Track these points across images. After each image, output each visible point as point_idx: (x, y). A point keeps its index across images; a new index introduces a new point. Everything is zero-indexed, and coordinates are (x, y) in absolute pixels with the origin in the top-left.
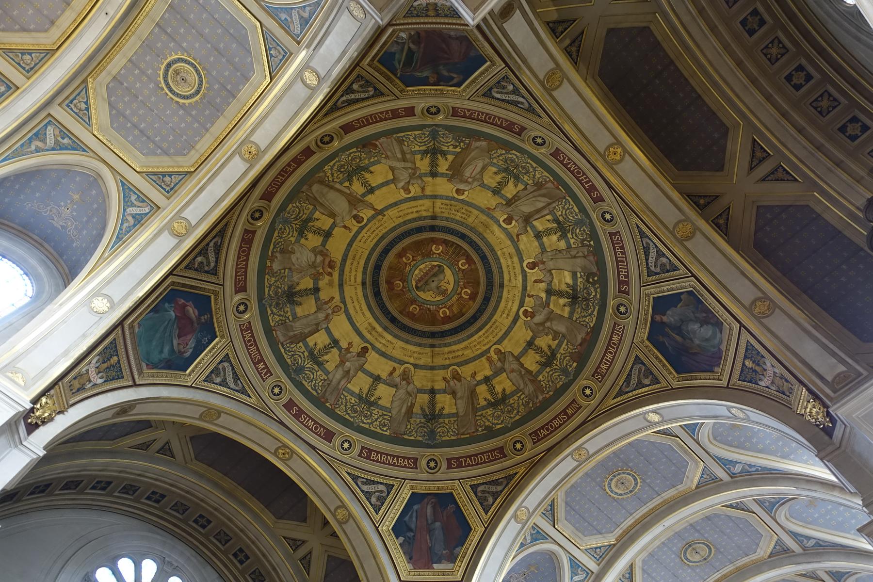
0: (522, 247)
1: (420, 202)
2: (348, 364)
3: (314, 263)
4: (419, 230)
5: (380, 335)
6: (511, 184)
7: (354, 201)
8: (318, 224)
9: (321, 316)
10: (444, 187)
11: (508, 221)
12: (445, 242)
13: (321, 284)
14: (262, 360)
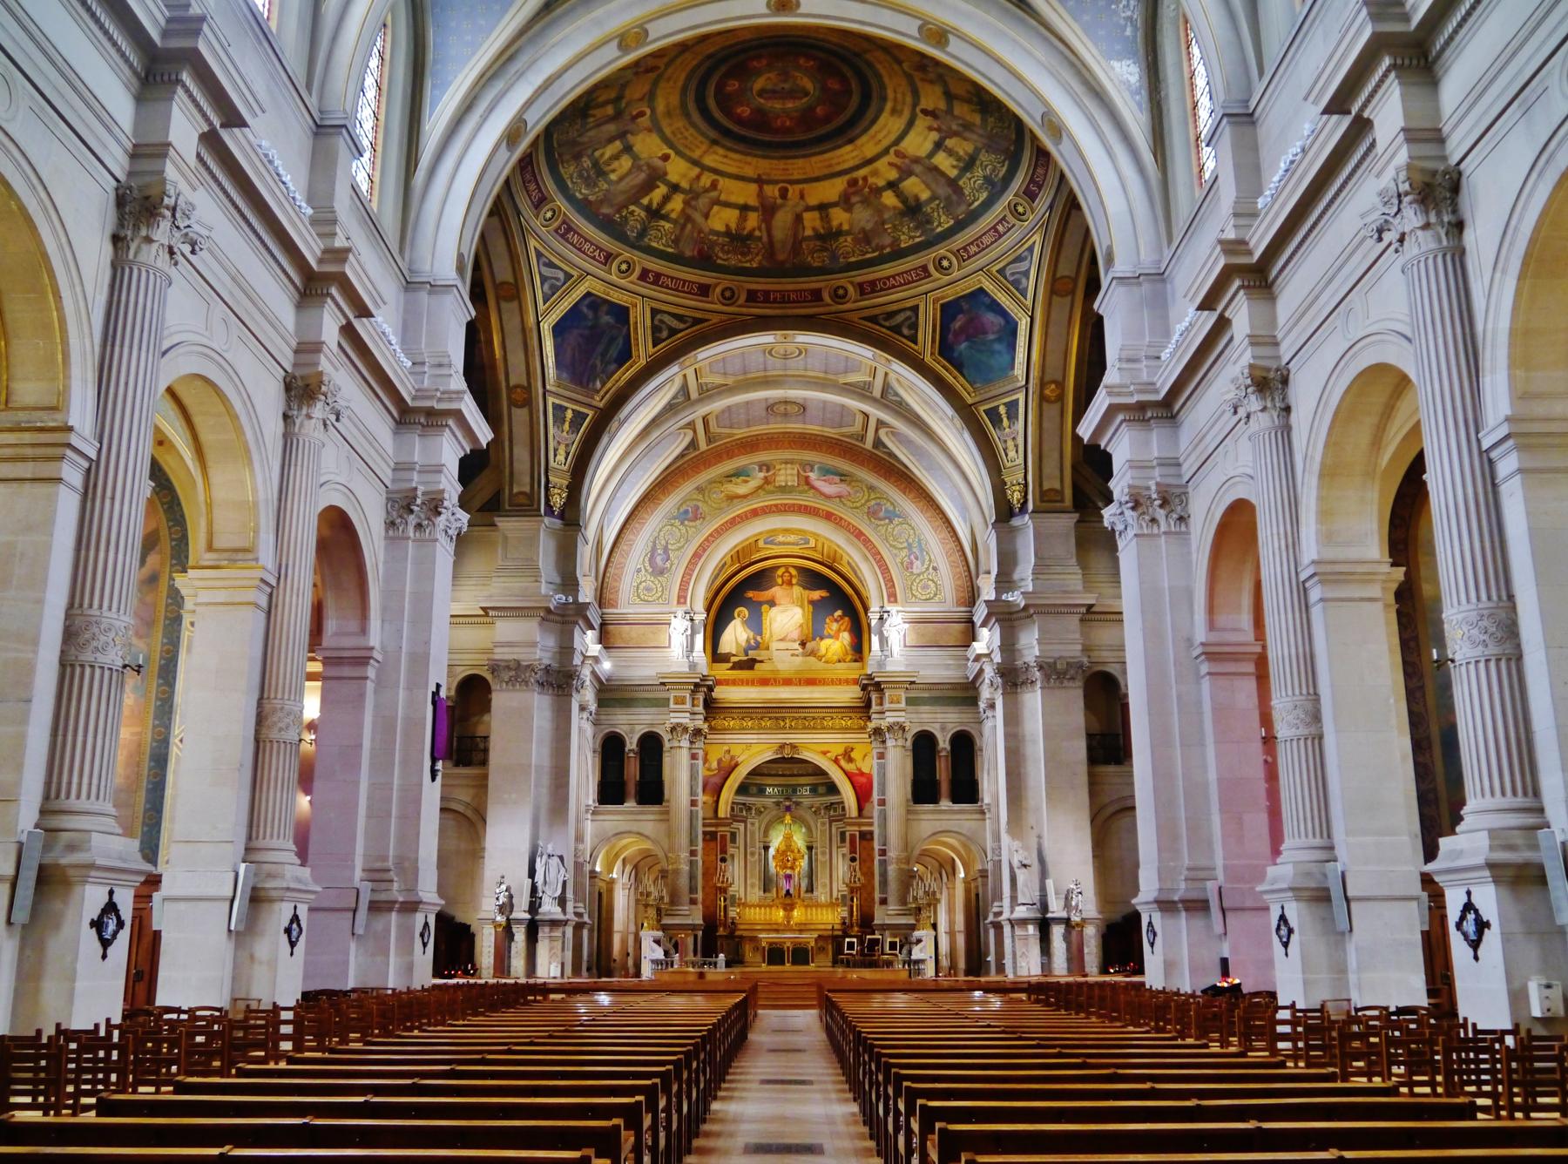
0: (646, 88)
1: (712, 164)
2: (954, 127)
3: (862, 202)
4: (742, 139)
5: (895, 100)
6: (607, 156)
7: (768, 211)
8: (818, 224)
9: (918, 169)
10: (678, 170)
11: (642, 114)
12: (728, 113)
13: (881, 183)
14: (994, 228)
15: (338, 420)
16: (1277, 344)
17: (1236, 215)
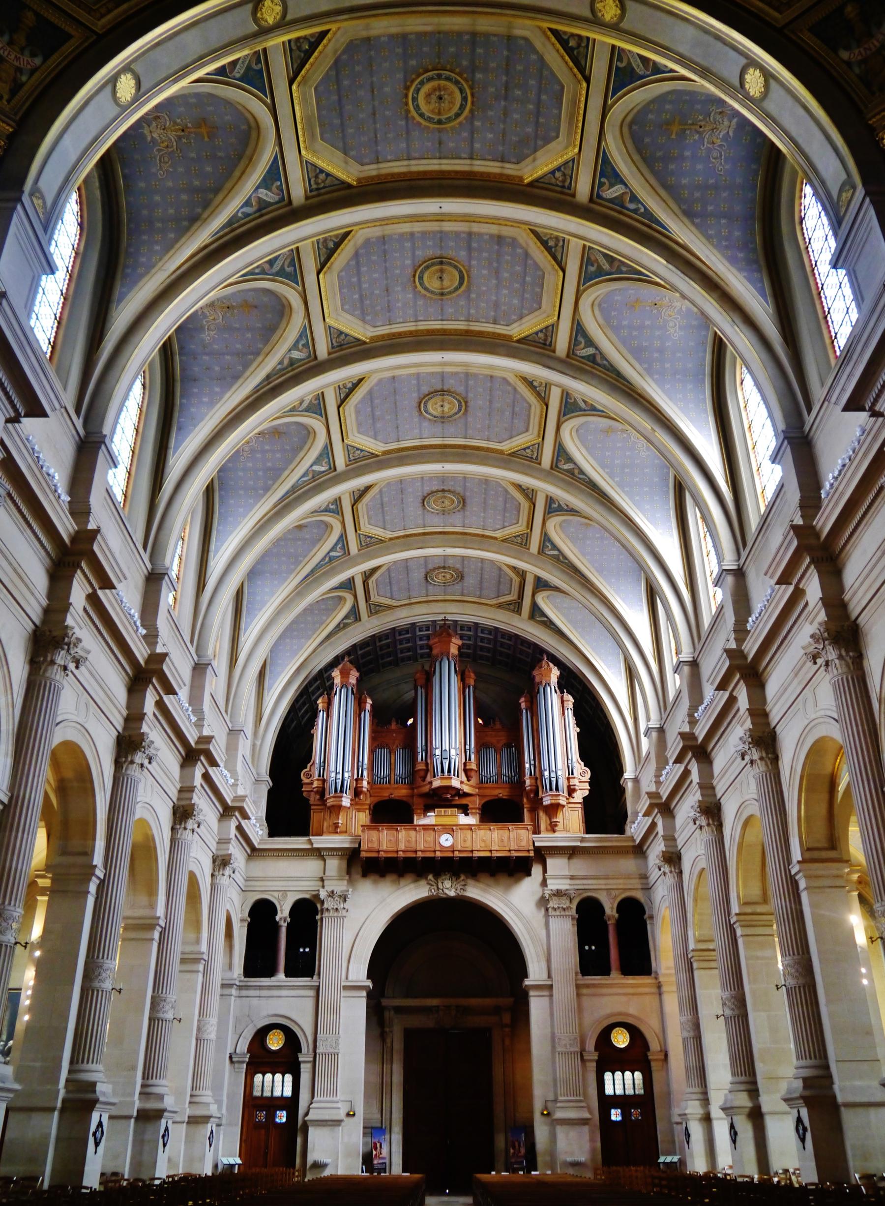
15: (198, 827)
16: (675, 840)
17: (735, 631)
